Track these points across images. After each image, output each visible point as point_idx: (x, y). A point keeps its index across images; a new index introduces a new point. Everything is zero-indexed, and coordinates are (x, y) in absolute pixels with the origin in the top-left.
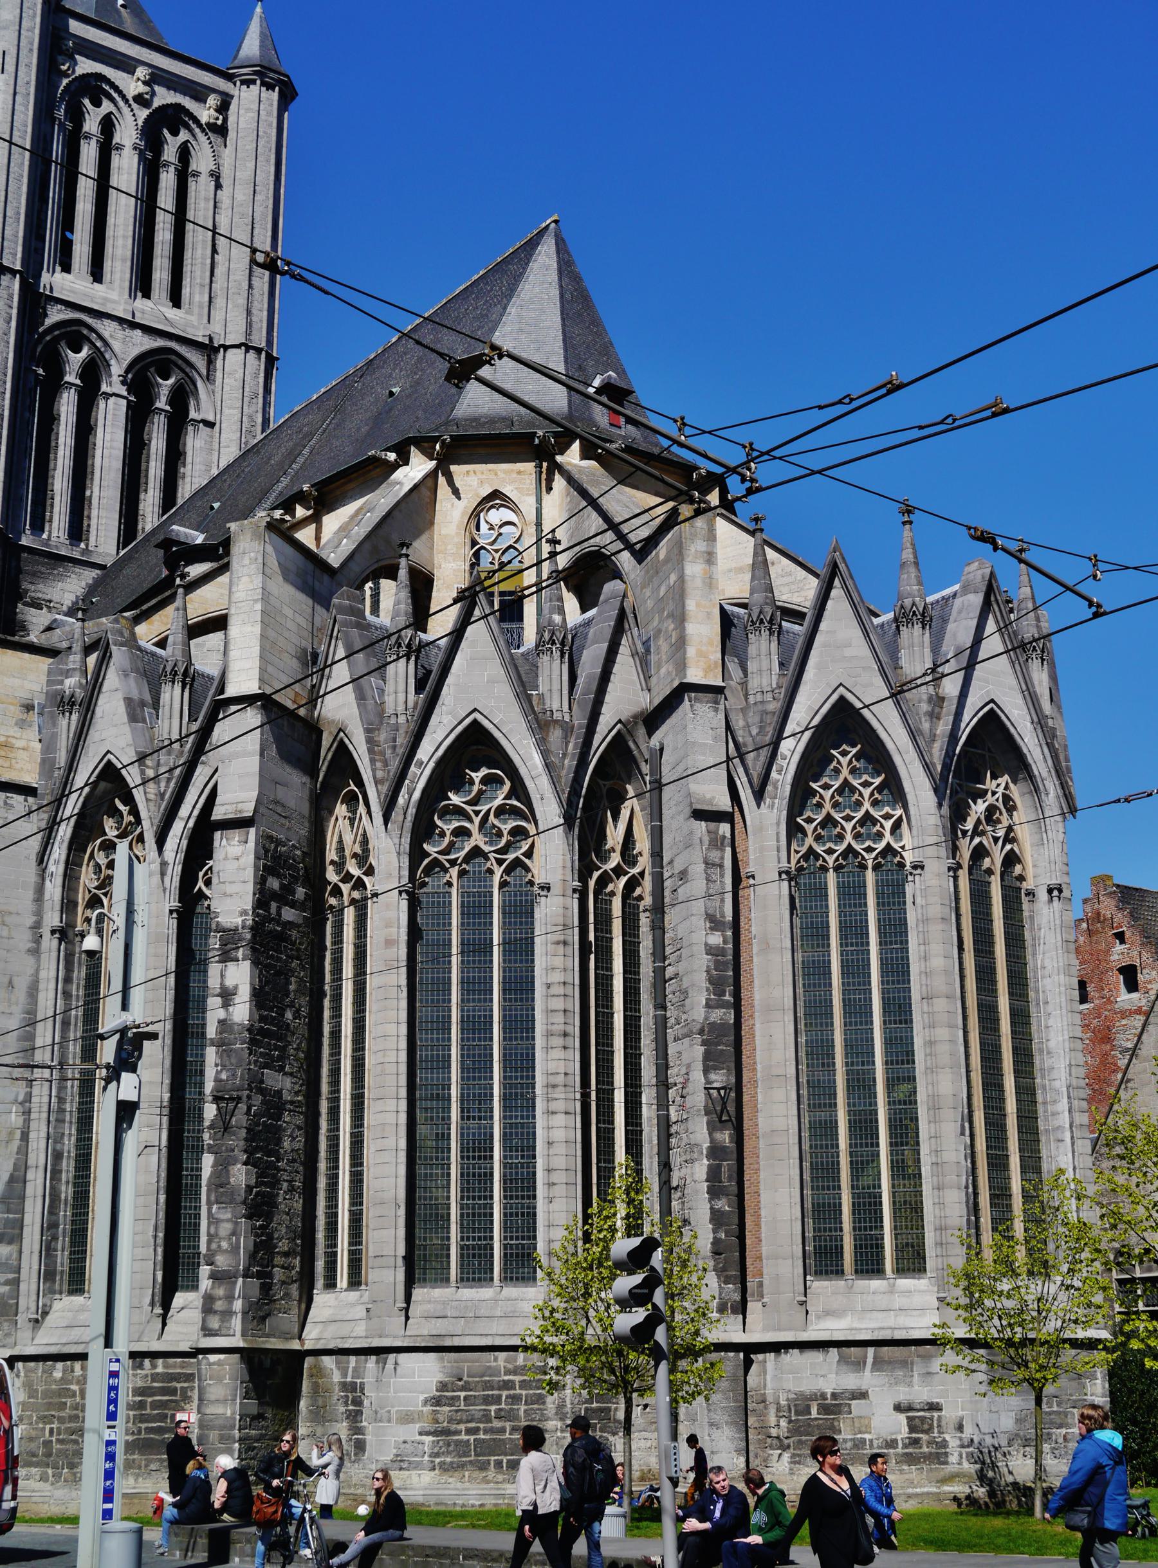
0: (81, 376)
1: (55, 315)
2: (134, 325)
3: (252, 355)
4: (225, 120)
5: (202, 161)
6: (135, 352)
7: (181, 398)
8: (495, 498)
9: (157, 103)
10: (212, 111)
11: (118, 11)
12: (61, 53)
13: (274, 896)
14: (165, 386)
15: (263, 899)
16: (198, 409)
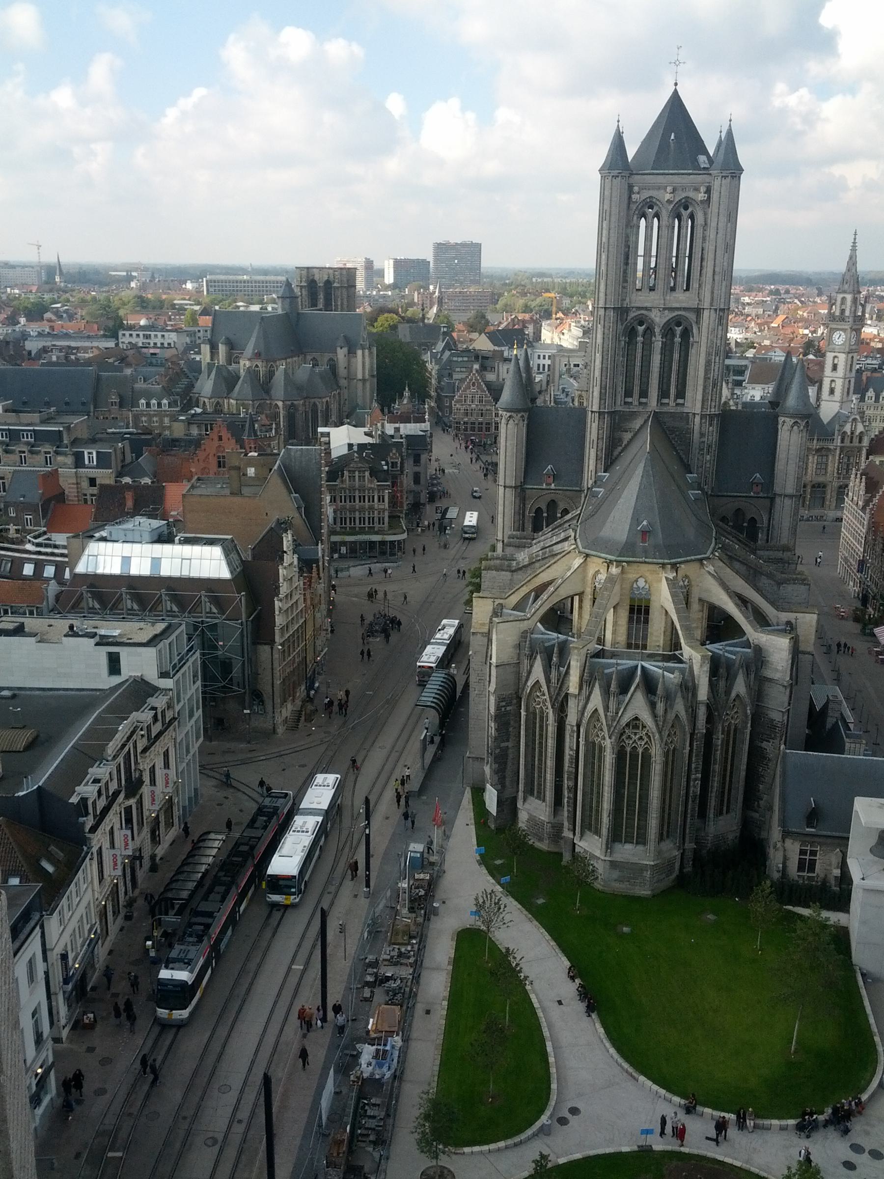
0: (643, 336)
1: (632, 315)
2: (665, 309)
3: (712, 311)
4: (709, 197)
5: (700, 219)
6: (665, 320)
7: (686, 334)
8: (598, 572)
9: (677, 200)
10: (702, 194)
11: (669, 146)
12: (634, 193)
13: (504, 706)
14: (678, 330)
15: (498, 708)
16: (693, 337)
